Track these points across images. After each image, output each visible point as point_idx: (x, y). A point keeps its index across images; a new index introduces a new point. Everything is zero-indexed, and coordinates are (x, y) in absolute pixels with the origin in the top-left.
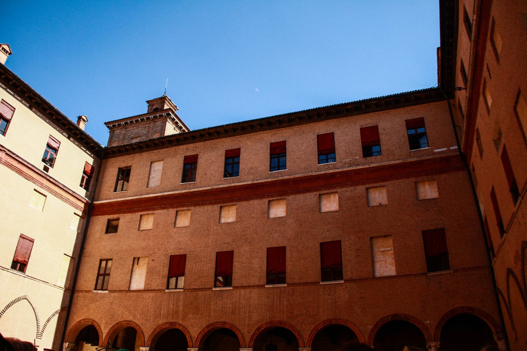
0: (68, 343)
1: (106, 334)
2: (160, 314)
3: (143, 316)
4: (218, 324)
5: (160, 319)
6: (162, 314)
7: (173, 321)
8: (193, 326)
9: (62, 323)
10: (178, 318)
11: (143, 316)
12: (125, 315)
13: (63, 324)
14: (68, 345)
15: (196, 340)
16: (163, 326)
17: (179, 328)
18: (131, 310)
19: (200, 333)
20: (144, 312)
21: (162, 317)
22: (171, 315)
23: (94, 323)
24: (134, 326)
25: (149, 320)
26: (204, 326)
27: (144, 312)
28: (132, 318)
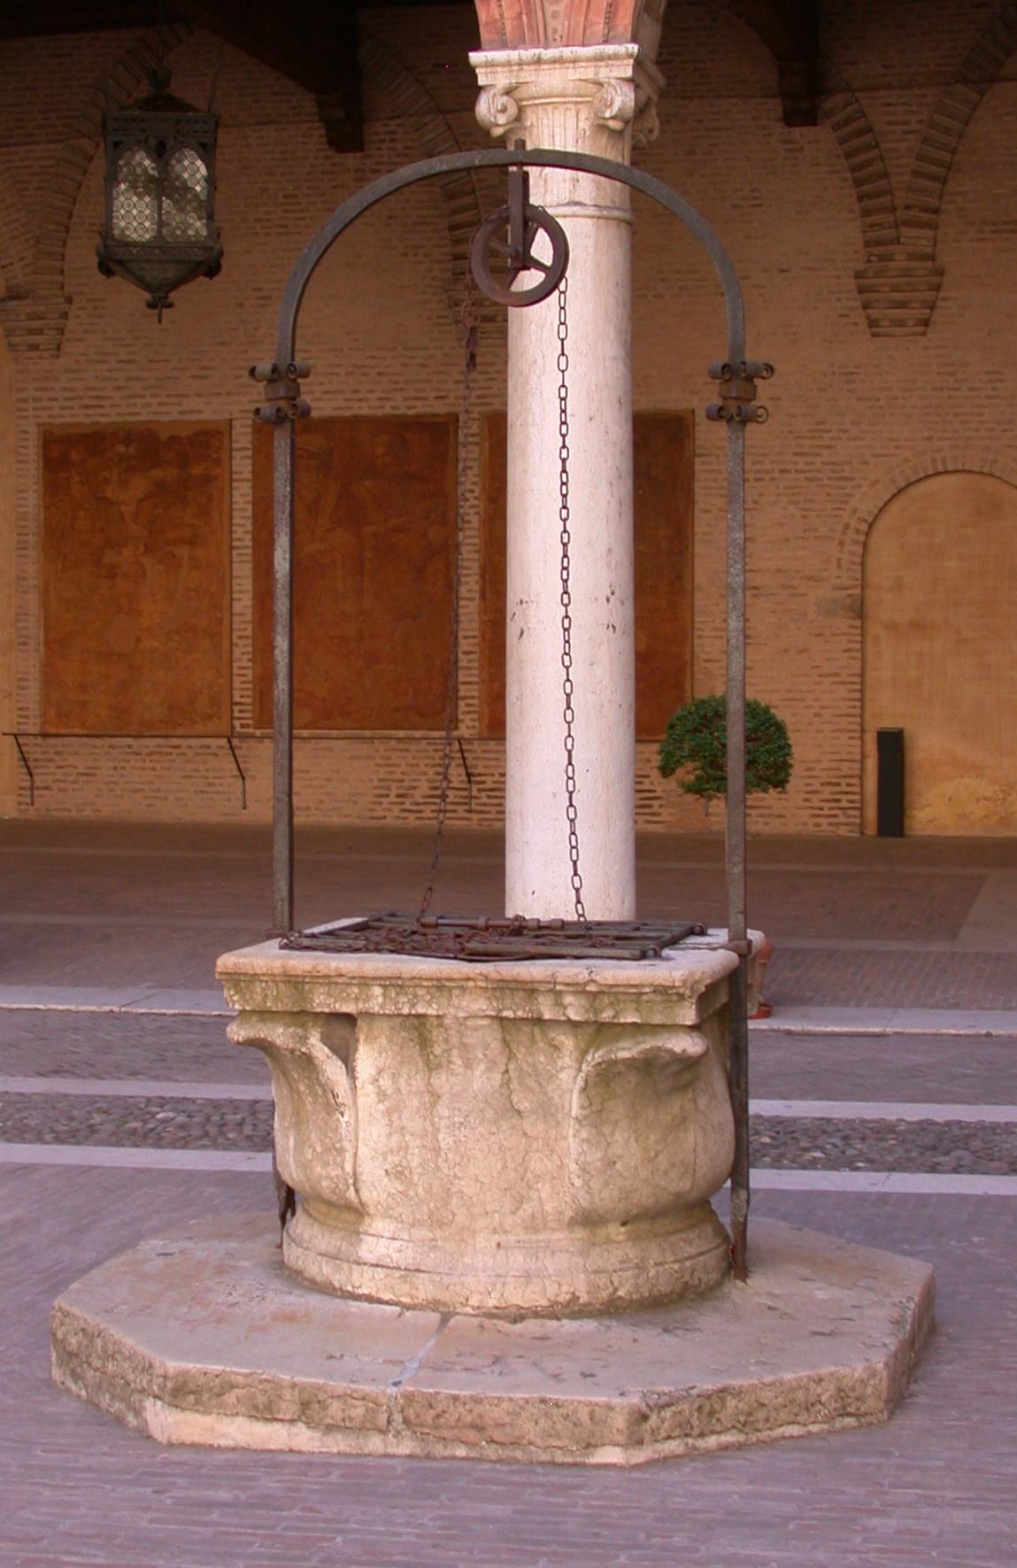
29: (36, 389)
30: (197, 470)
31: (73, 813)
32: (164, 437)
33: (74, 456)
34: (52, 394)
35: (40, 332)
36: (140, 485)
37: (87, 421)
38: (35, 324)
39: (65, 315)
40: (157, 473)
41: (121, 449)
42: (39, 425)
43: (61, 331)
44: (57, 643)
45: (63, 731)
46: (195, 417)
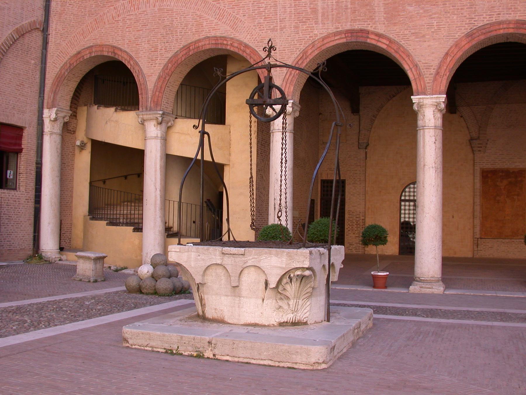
0: (55, 110)
1: (156, 77)
2: (314, 11)
3: (262, 21)
4: (501, 27)
5: (316, 23)
6: (320, 11)
7: (357, 26)
8: (424, 36)
9: (33, 62)
10: (371, 18)
11: (262, 21)
12: (205, 24)
13: (35, 64)
14: (56, 114)
15: (437, 73)
16: (325, 42)
17: (379, 44)
18: (222, 7)
19: (447, 54)
20: (262, 10)
21: (320, 18)
22: (349, 11)
23: (119, 53)
24: (236, 50)
25: (282, 29)
26: (458, 35)
27: (262, 10)
28: (229, 28)
29: (480, 160)
30: (519, 179)
31: (488, 256)
32: (511, 171)
33: (489, 175)
34: (484, 161)
35: (481, 147)
36: (505, 182)
37: (492, 167)
38: (480, 146)
39: (487, 144)
40: (510, 180)
41: (501, 174)
42: (480, 168)
43: (486, 147)
44: (485, 218)
45: (486, 237)
46: (518, 167)
